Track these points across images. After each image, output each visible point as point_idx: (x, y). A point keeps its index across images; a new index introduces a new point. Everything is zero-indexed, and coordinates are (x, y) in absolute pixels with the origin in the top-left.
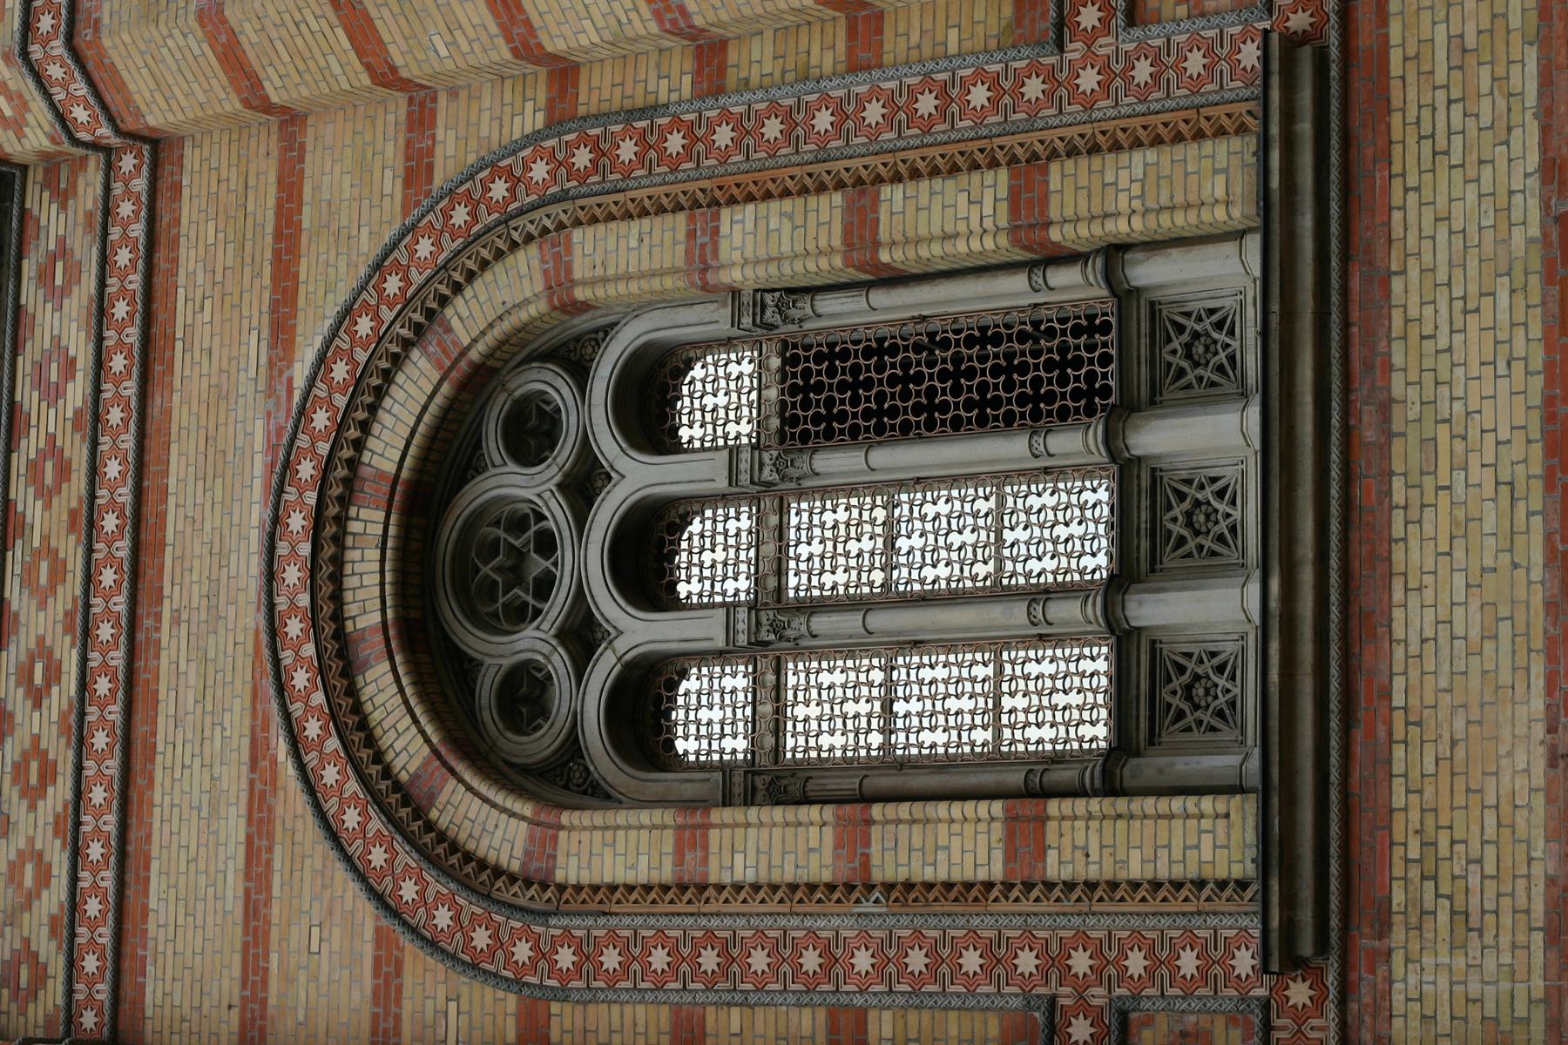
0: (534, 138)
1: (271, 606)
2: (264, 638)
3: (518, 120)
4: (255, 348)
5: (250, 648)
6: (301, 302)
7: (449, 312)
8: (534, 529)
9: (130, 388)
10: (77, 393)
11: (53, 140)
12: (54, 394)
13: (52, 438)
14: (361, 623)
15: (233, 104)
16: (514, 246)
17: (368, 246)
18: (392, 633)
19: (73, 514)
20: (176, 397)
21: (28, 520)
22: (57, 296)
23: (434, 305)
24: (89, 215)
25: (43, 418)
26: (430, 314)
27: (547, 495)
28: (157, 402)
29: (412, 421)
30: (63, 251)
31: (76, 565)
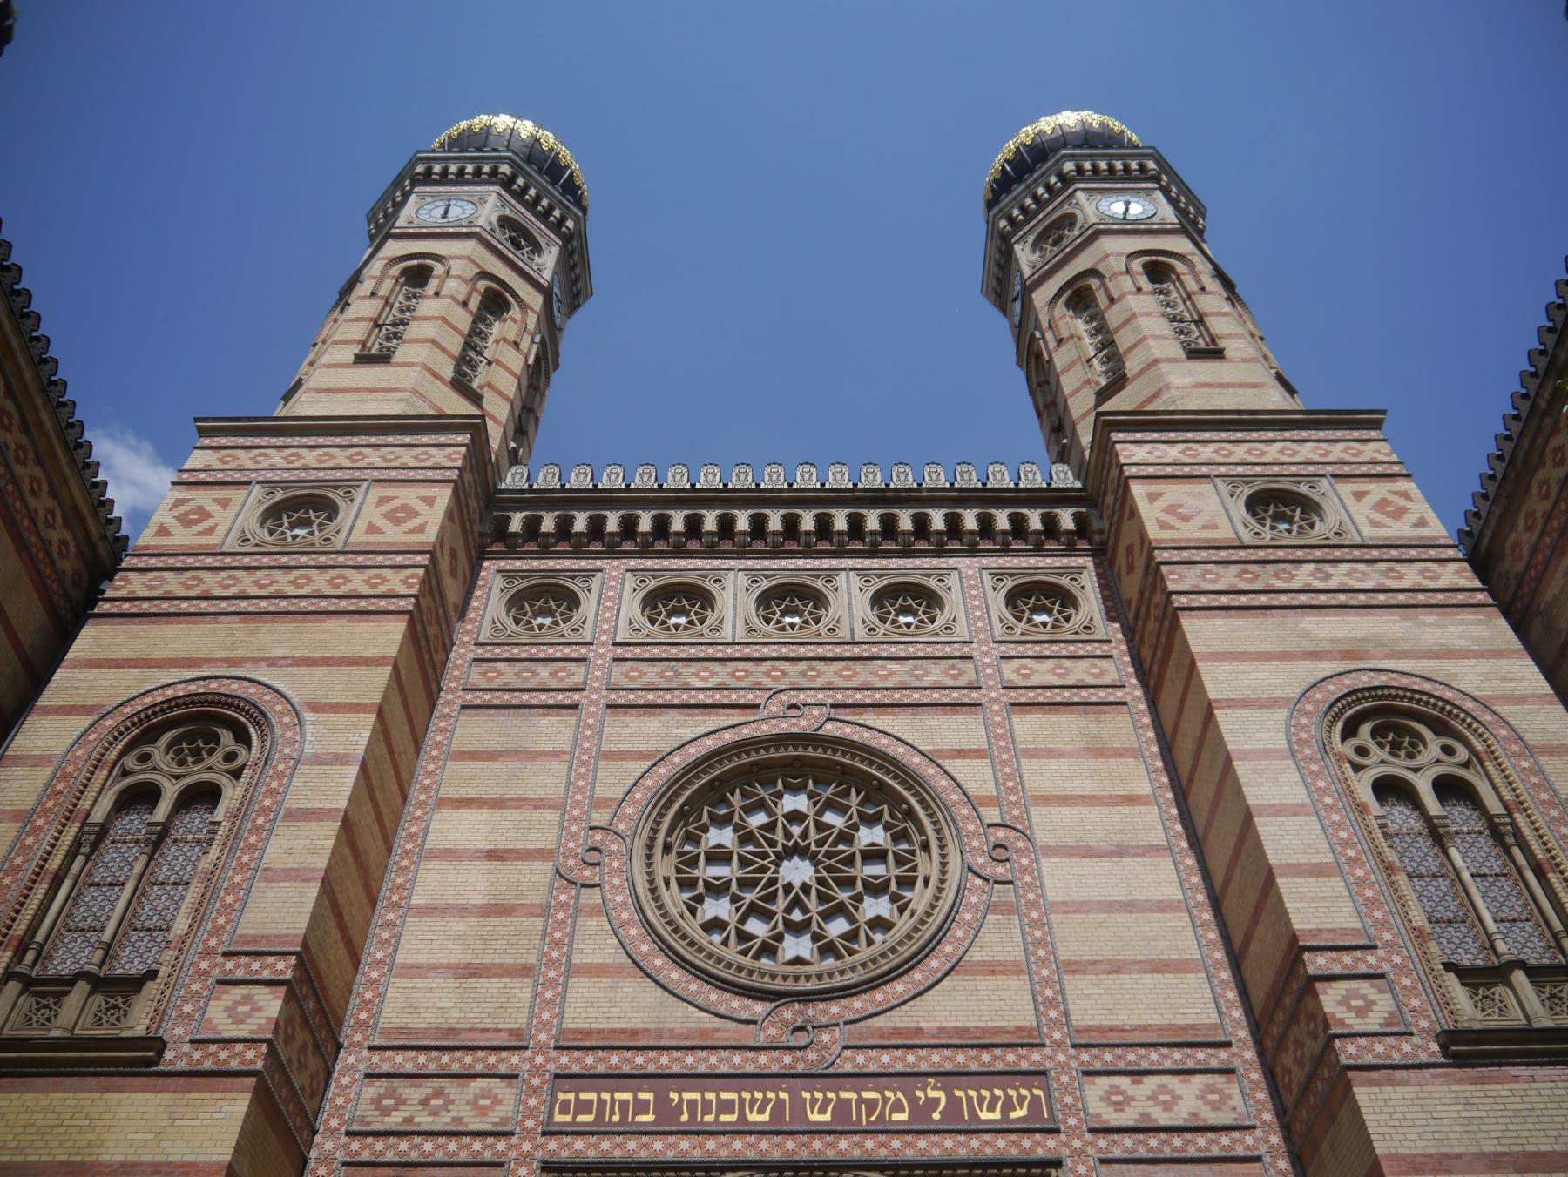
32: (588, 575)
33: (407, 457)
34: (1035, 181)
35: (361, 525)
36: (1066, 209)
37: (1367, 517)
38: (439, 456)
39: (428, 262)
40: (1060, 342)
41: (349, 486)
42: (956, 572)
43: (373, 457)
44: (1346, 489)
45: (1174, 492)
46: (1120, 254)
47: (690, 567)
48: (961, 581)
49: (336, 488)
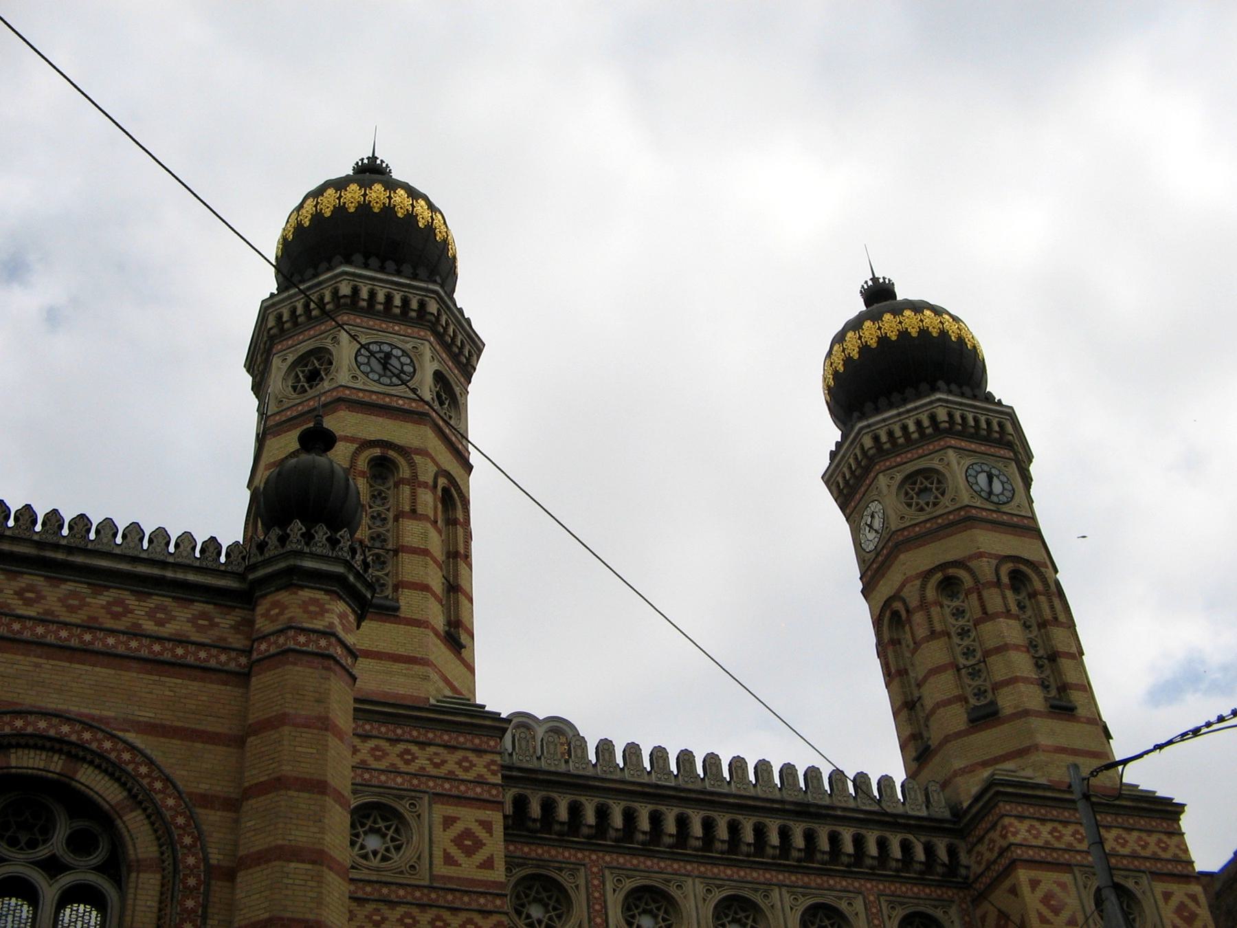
0: (206, 859)
1: (31, 713)
2: (18, 708)
3: (216, 851)
4: (146, 715)
5: (15, 700)
6: (162, 740)
7: (139, 811)
8: (40, 838)
9: (144, 653)
10: (149, 626)
11: (258, 630)
12: (151, 615)
13: (131, 612)
14: (13, 756)
15: (252, 719)
16: (160, 846)
17: (179, 775)
18: (5, 771)
19: (95, 619)
20: (135, 675)
21: (99, 597)
22: (193, 621)
23: (143, 806)
24: (225, 639)
25: (142, 608)
26: (140, 803)
27: (51, 848)
28: (134, 665)
29: (97, 789)
30: (213, 625)
31: (74, 619)
32: (574, 868)
33: (451, 762)
34: (908, 411)
35: (438, 853)
36: (935, 464)
37: (1172, 922)
38: (480, 766)
39: (392, 454)
40: (933, 632)
41: (413, 795)
42: (861, 897)
43: (422, 759)
44: (1159, 887)
45: (1049, 879)
46: (990, 555)
47: (652, 870)
48: (866, 909)
49: (401, 798)
